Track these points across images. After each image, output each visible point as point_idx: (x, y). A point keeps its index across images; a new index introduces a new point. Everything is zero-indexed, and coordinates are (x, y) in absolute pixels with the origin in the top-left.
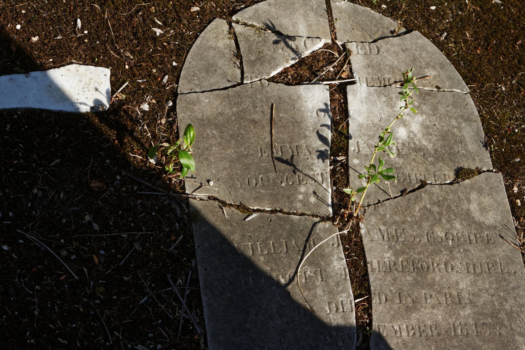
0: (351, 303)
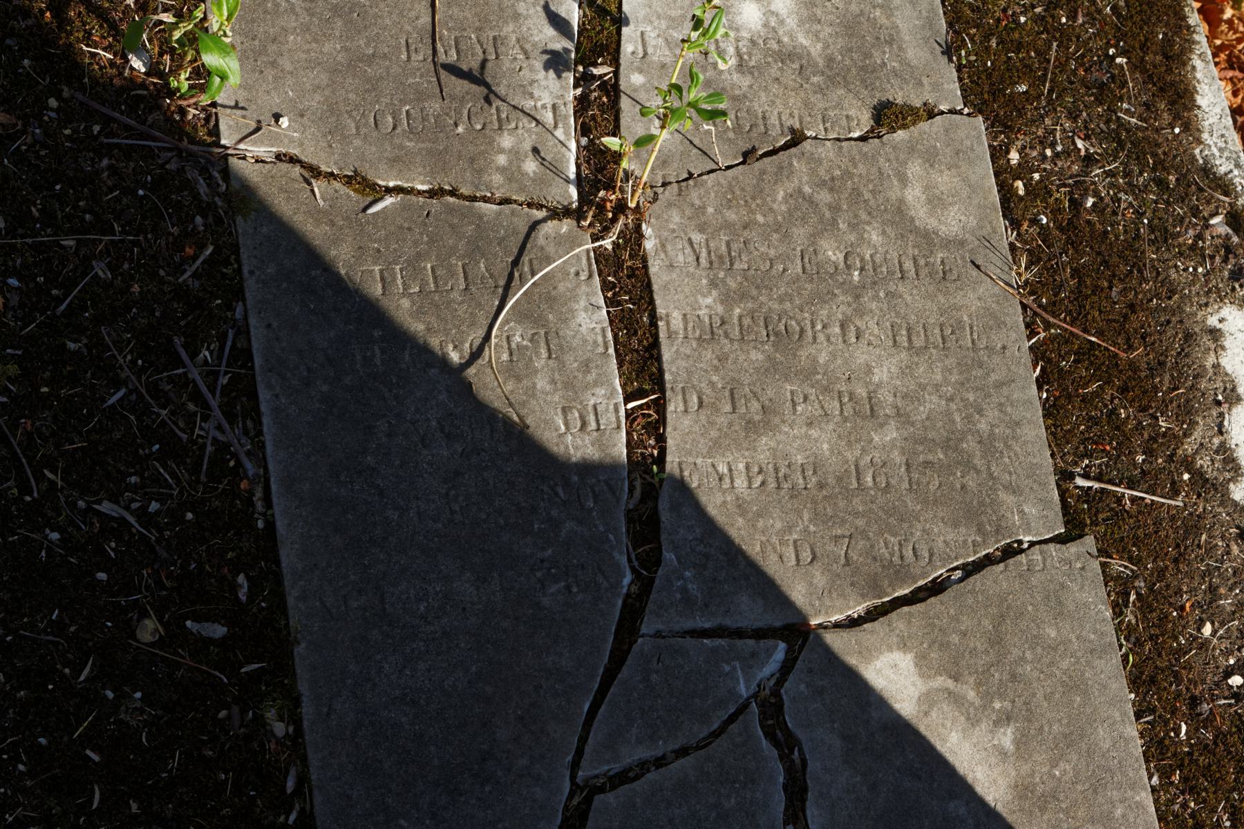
0: (617, 410)
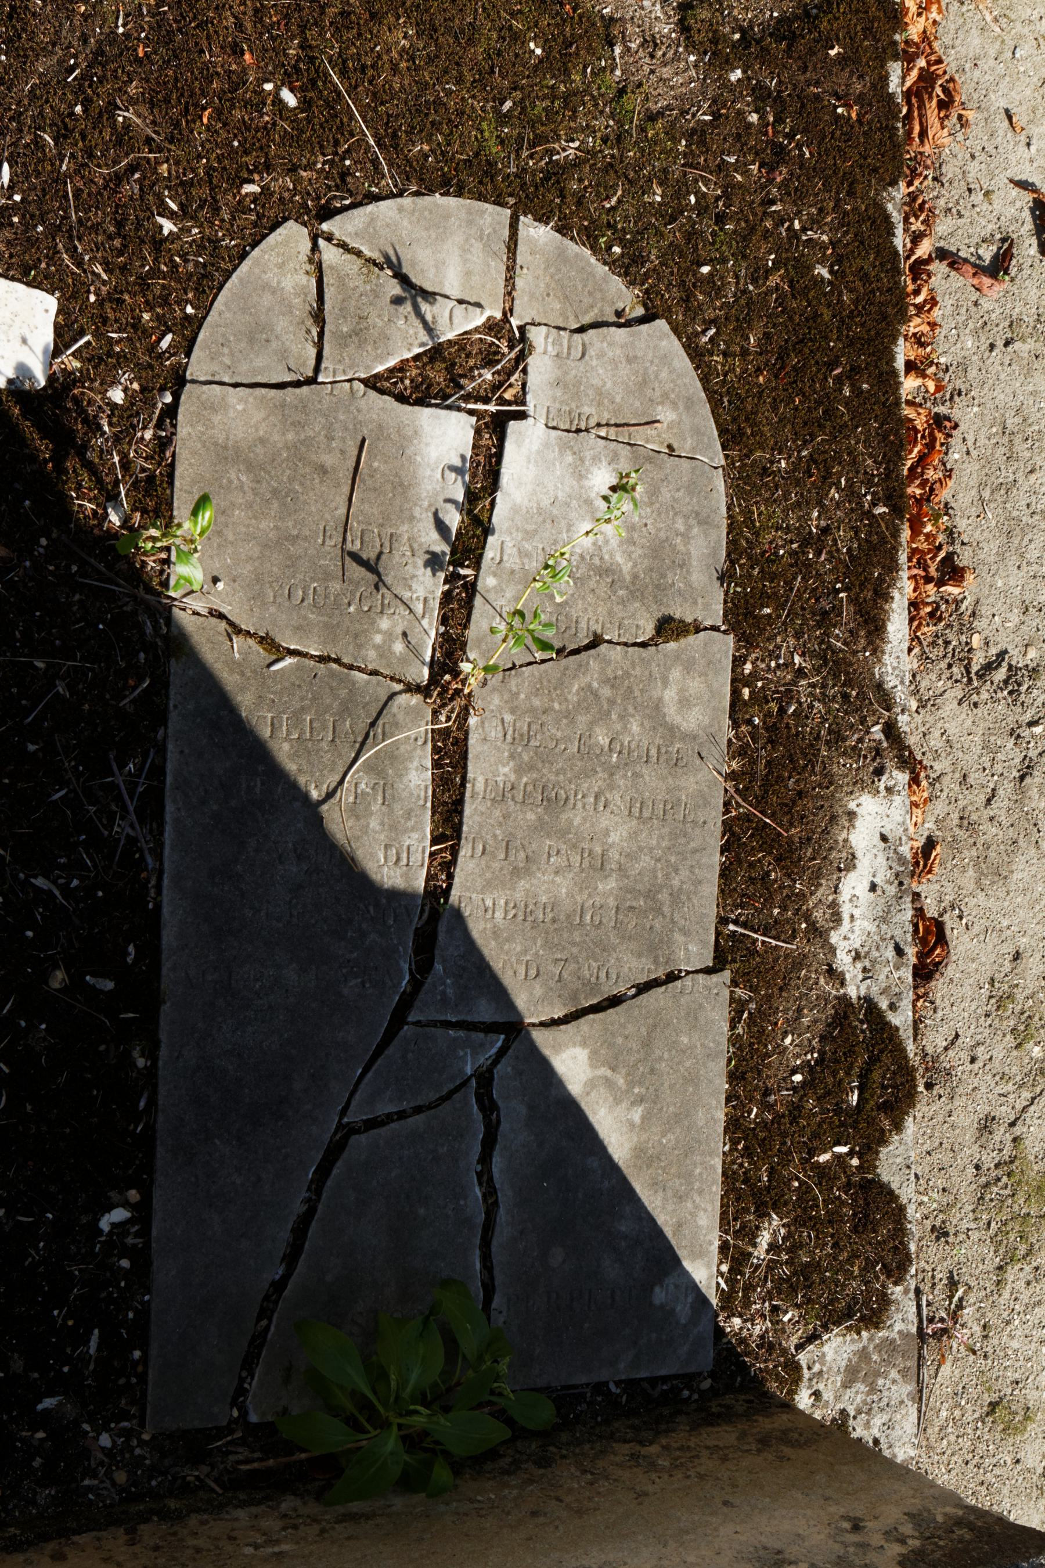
0: (423, 852)
